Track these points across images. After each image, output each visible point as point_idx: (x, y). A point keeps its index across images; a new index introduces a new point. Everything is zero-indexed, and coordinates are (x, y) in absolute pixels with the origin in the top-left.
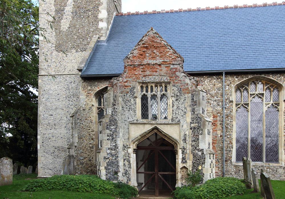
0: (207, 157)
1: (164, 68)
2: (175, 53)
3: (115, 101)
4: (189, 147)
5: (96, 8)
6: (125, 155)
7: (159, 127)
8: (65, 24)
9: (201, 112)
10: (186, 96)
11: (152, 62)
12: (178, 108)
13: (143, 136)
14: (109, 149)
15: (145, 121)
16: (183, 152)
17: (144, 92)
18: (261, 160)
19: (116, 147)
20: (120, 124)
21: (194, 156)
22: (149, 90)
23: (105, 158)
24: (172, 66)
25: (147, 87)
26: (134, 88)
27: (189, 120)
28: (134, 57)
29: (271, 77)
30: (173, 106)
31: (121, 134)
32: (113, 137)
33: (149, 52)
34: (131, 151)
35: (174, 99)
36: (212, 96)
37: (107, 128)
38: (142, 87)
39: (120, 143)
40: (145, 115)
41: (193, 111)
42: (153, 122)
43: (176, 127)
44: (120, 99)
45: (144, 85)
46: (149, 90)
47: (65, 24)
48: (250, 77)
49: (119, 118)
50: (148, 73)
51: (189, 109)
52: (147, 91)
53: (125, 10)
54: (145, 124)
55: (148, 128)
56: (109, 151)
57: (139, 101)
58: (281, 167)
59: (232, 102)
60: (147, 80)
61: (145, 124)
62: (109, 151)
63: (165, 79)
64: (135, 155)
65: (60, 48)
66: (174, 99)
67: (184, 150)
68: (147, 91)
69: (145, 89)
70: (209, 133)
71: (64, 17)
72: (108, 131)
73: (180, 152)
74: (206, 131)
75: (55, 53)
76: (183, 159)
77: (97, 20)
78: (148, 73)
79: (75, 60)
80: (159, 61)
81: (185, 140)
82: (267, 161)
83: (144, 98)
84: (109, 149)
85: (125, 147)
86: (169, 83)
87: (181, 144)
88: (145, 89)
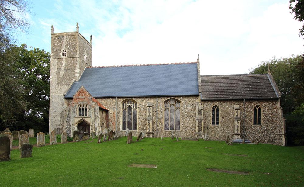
0: (97, 128)
1: (86, 99)
2: (89, 94)
3: (69, 110)
4: (93, 125)
5: (75, 68)
6: (73, 128)
7: (84, 118)
8: (61, 74)
9: (96, 114)
10: (93, 108)
11: (82, 97)
12: (90, 112)
13: (79, 121)
14: (67, 126)
15: (79, 116)
16: (92, 127)
17: (80, 107)
18: (131, 129)
19: (70, 125)
20: (71, 117)
21: (95, 128)
22: (81, 106)
23: (65, 129)
24: (88, 99)
25: (80, 105)
26: (76, 106)
27: (93, 116)
28: (76, 95)
29: (133, 99)
30: (88, 111)
31: (72, 121)
32: (68, 122)
33: (81, 94)
34: (75, 126)
35: (89, 109)
36: (113, 106)
37: (66, 119)
38: (79, 105)
39: (71, 124)
40: (80, 115)
41: (94, 113)
42: (82, 117)
43: (89, 118)
44: (72, 109)
45: (79, 105)
46: (81, 106)
47: (61, 74)
48: (126, 99)
49: (71, 115)
50: (80, 101)
51: (93, 113)
52: (80, 107)
53: (95, 63)
54: (79, 117)
55: (81, 119)
56: (67, 127)
57: (78, 110)
58: (137, 132)
59: (120, 108)
60: (80, 103)
61: (79, 117)
62: (67, 127)
63: (86, 103)
64: (77, 128)
65: (59, 84)
66: (89, 109)
67: (92, 126)
68: (80, 107)
69: (80, 106)
70: (98, 120)
71: (61, 71)
72: (66, 120)
73: (91, 126)
74: (97, 120)
75: (57, 86)
76: (92, 129)
77: (75, 73)
78: (80, 101)
79: (64, 89)
80: (84, 97)
81: (92, 123)
82: (133, 130)
83: (80, 109)
84: (67, 126)
85: (73, 125)
86: (87, 104)
87: (91, 124)
88: (80, 106)
